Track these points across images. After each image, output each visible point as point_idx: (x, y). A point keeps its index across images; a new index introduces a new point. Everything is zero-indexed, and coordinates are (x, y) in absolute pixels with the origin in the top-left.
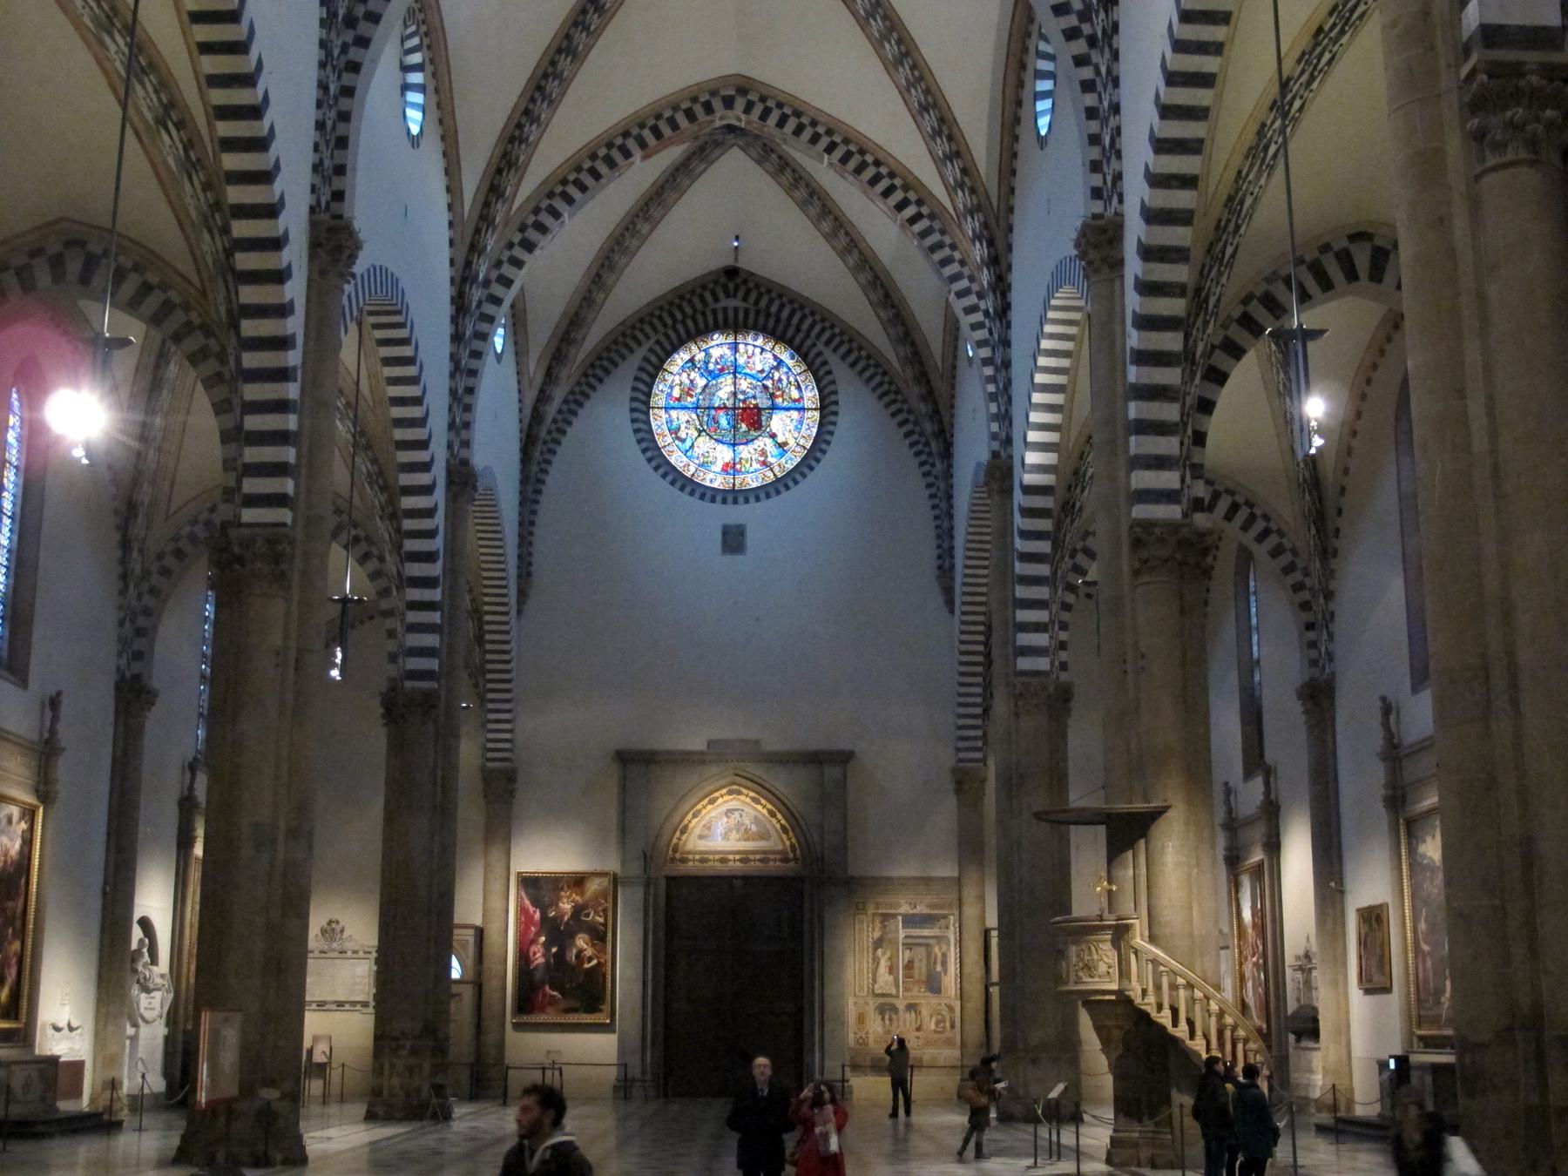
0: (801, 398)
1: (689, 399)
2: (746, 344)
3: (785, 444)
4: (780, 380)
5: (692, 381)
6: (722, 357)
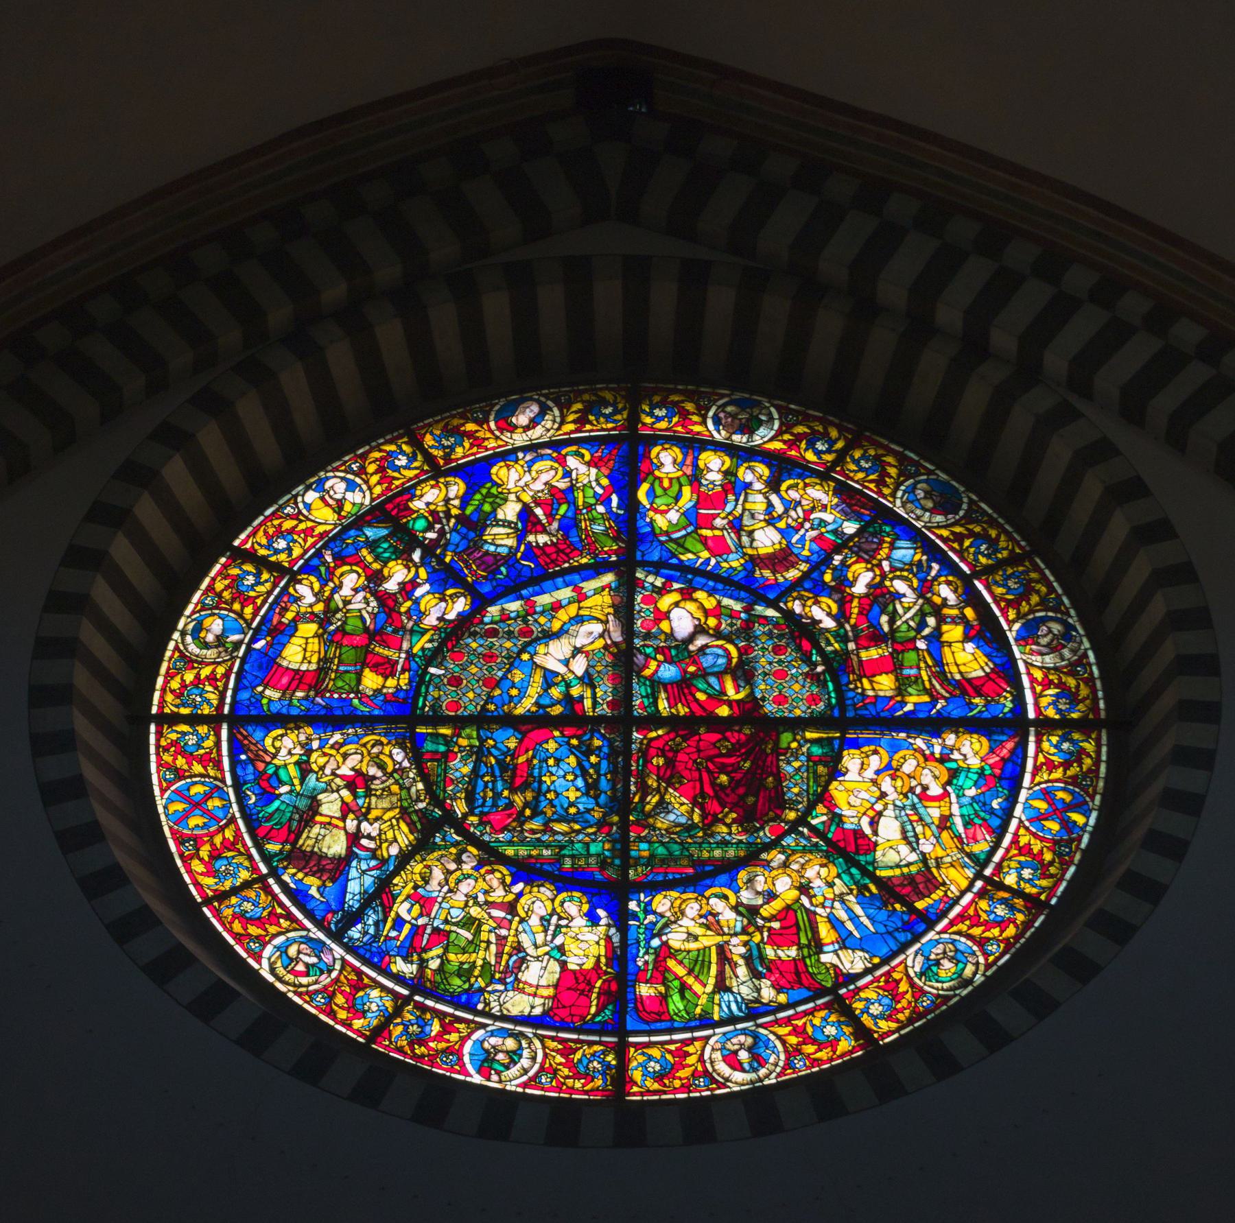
0: (1006, 671)
1: (371, 681)
2: (693, 445)
3: (926, 879)
4: (880, 596)
5: (387, 602)
6: (556, 497)
